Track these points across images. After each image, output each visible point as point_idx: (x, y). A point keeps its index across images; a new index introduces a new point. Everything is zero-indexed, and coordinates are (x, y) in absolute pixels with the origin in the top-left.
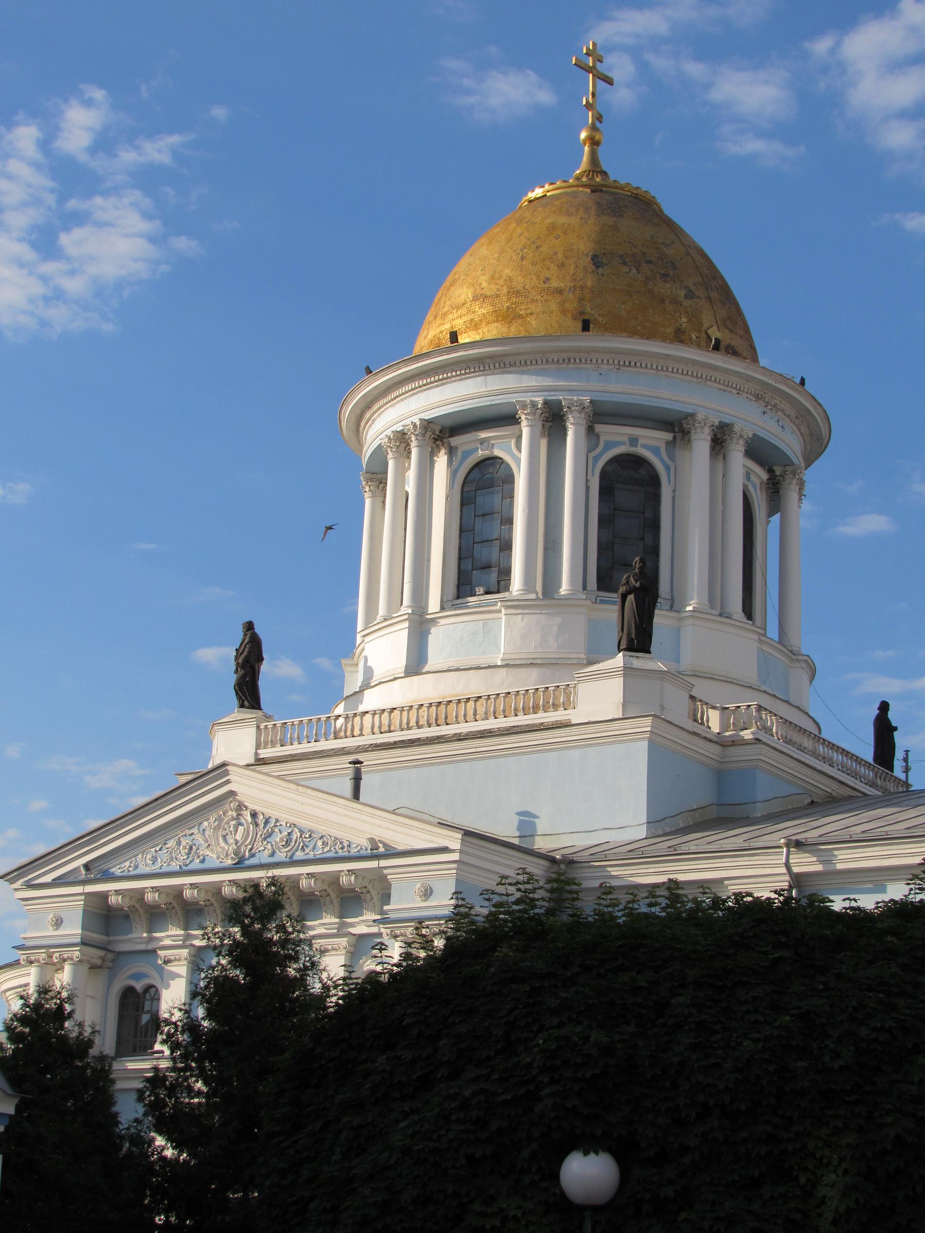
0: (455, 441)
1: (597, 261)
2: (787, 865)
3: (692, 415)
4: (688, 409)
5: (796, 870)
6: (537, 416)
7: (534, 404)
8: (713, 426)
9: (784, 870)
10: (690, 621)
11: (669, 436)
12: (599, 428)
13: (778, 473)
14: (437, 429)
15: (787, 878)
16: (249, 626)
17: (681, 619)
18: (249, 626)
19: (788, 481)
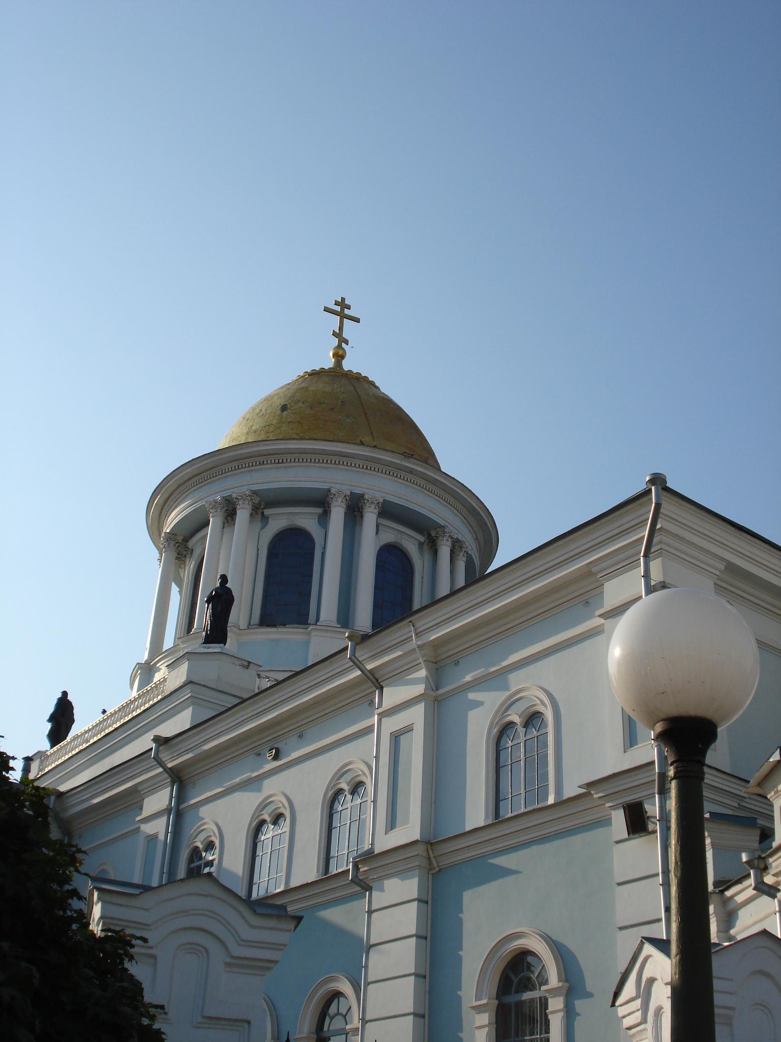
0: (191, 544)
1: (284, 408)
2: (161, 764)
3: (329, 490)
4: (326, 486)
5: (170, 765)
6: (219, 510)
7: (216, 502)
8: (345, 496)
9: (161, 770)
10: (314, 633)
11: (319, 511)
12: (267, 512)
13: (433, 534)
14: (180, 538)
15: (166, 775)
16: (65, 694)
17: (309, 634)
18: (65, 694)
19: (441, 538)
